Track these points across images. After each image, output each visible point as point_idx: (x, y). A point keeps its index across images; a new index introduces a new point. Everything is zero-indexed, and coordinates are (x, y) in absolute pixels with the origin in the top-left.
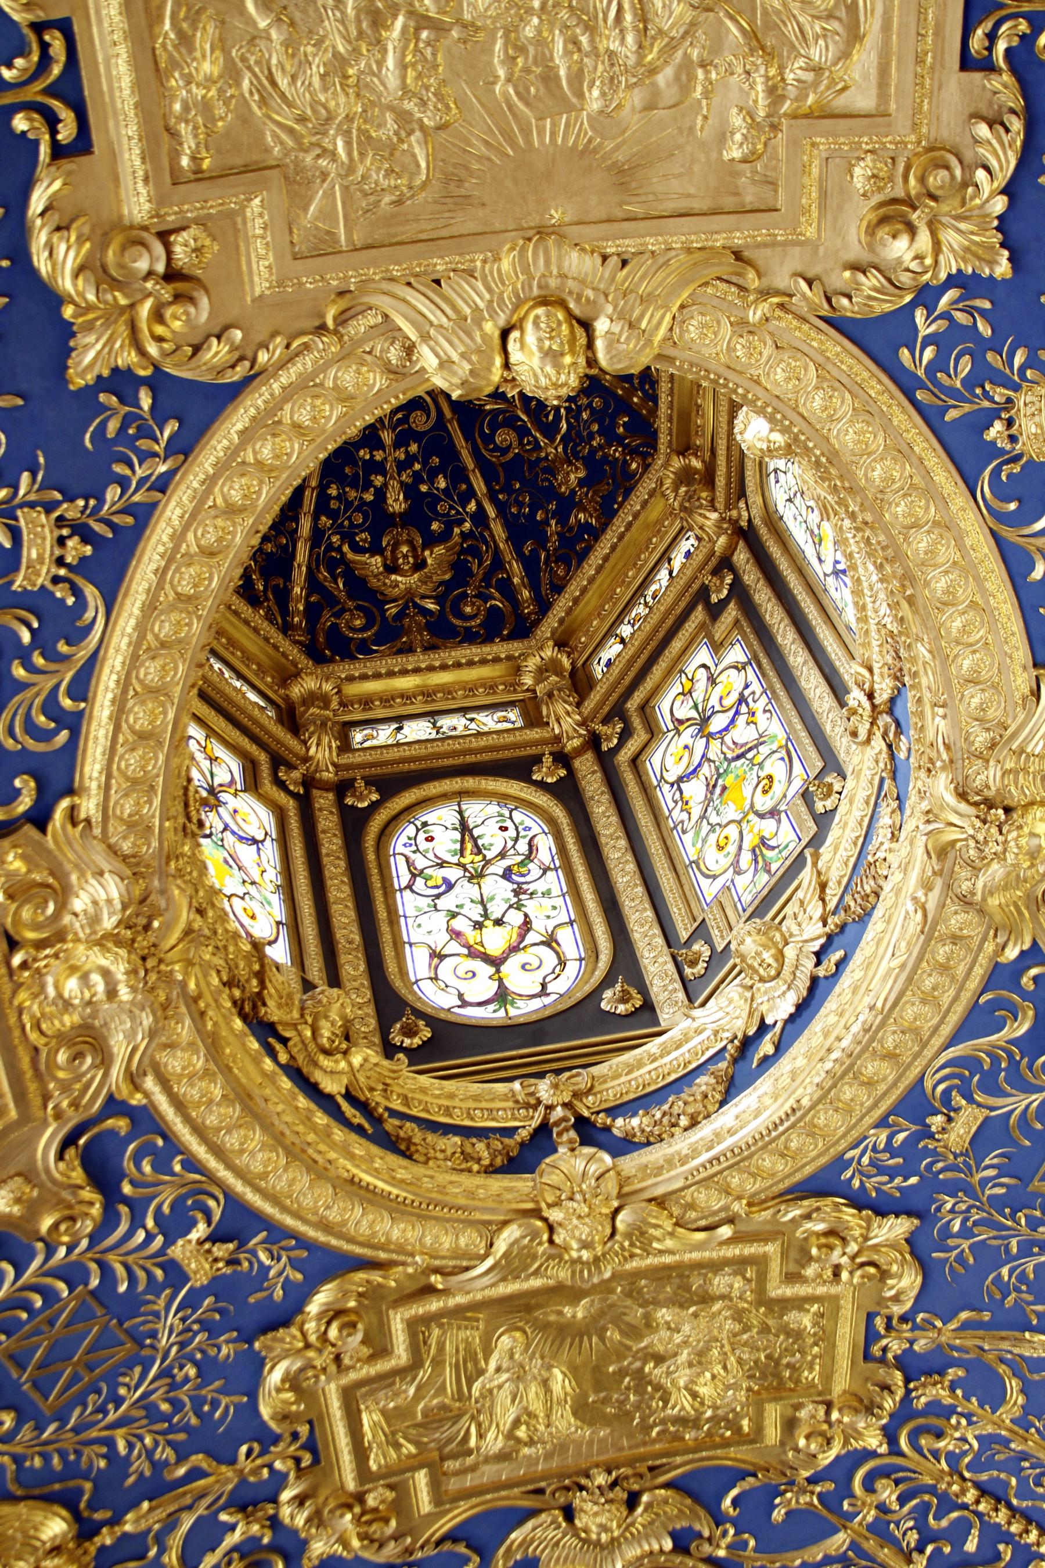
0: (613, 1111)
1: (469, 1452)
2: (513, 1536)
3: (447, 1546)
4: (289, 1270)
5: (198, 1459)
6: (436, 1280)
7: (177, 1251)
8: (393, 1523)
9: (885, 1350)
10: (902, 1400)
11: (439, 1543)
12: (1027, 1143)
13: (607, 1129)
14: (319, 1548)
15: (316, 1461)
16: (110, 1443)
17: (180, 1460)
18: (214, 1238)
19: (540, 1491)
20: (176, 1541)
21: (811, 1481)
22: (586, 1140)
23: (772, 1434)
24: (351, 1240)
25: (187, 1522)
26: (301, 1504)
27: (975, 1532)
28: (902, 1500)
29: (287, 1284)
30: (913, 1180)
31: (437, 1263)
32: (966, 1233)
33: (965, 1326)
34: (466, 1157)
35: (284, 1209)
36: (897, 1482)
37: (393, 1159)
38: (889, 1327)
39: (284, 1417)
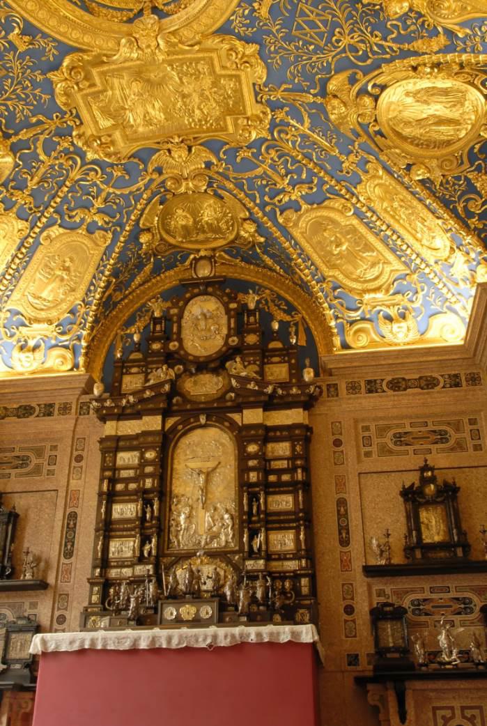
0: (164, 5)
1: (132, 126)
2: (153, 158)
3: (132, 159)
4: (53, 50)
5: (41, 118)
6: (105, 59)
7: (11, 37)
8: (112, 149)
9: (262, 98)
10: (271, 120)
11: (129, 158)
12: (287, 15)
13: (162, 10)
14: (90, 156)
15: (82, 123)
16: (6, 106)
17: (33, 116)
18: (23, 33)
19: (158, 143)
20: (40, 144)
21: (249, 147)
22: (153, 13)
23: (231, 129)
24: (70, 39)
25: (42, 138)
26: (80, 138)
27: (305, 172)
28: (279, 157)
29: (53, 54)
30: (255, 29)
31: (105, 52)
32: (276, 52)
33: (285, 90)
34: (113, 17)
35: (43, 25)
36: (277, 151)
37: (83, 13)
38: (260, 89)
39: (65, 104)
